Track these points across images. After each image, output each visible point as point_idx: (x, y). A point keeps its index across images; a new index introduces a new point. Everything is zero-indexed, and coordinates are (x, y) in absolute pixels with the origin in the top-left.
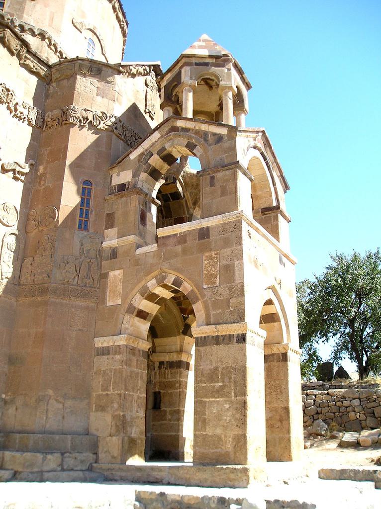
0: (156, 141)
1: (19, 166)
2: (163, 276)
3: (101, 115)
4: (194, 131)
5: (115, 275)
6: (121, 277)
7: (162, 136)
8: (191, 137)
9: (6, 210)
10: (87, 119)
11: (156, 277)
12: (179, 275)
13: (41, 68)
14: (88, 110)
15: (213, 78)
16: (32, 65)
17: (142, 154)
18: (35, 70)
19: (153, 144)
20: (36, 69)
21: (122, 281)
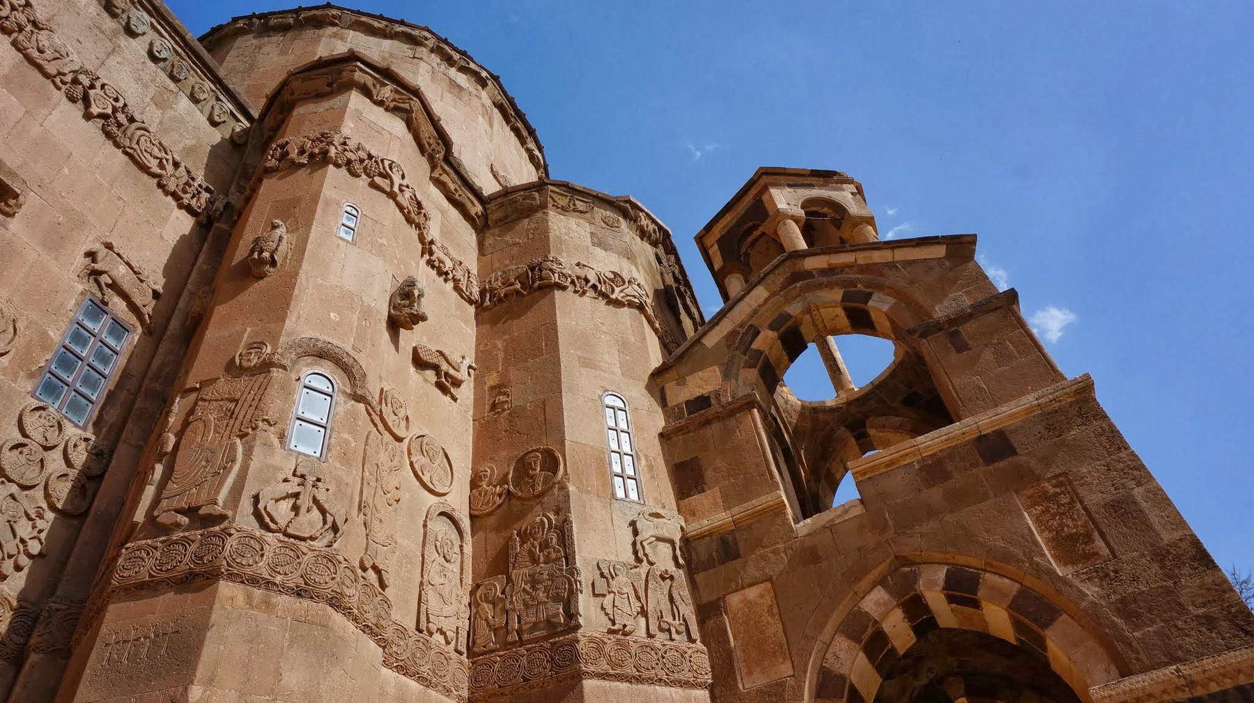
0: (760, 306)
1: (448, 361)
2: (905, 575)
3: (612, 276)
4: (855, 269)
5: (747, 602)
6: (768, 600)
7: (773, 294)
8: (853, 283)
9: (425, 453)
10: (587, 281)
11: (882, 582)
12: (961, 560)
13: (468, 198)
14: (584, 266)
15: (825, 210)
16: (452, 187)
17: (733, 334)
18: (457, 197)
19: (755, 312)
20: (460, 195)
21: (775, 610)
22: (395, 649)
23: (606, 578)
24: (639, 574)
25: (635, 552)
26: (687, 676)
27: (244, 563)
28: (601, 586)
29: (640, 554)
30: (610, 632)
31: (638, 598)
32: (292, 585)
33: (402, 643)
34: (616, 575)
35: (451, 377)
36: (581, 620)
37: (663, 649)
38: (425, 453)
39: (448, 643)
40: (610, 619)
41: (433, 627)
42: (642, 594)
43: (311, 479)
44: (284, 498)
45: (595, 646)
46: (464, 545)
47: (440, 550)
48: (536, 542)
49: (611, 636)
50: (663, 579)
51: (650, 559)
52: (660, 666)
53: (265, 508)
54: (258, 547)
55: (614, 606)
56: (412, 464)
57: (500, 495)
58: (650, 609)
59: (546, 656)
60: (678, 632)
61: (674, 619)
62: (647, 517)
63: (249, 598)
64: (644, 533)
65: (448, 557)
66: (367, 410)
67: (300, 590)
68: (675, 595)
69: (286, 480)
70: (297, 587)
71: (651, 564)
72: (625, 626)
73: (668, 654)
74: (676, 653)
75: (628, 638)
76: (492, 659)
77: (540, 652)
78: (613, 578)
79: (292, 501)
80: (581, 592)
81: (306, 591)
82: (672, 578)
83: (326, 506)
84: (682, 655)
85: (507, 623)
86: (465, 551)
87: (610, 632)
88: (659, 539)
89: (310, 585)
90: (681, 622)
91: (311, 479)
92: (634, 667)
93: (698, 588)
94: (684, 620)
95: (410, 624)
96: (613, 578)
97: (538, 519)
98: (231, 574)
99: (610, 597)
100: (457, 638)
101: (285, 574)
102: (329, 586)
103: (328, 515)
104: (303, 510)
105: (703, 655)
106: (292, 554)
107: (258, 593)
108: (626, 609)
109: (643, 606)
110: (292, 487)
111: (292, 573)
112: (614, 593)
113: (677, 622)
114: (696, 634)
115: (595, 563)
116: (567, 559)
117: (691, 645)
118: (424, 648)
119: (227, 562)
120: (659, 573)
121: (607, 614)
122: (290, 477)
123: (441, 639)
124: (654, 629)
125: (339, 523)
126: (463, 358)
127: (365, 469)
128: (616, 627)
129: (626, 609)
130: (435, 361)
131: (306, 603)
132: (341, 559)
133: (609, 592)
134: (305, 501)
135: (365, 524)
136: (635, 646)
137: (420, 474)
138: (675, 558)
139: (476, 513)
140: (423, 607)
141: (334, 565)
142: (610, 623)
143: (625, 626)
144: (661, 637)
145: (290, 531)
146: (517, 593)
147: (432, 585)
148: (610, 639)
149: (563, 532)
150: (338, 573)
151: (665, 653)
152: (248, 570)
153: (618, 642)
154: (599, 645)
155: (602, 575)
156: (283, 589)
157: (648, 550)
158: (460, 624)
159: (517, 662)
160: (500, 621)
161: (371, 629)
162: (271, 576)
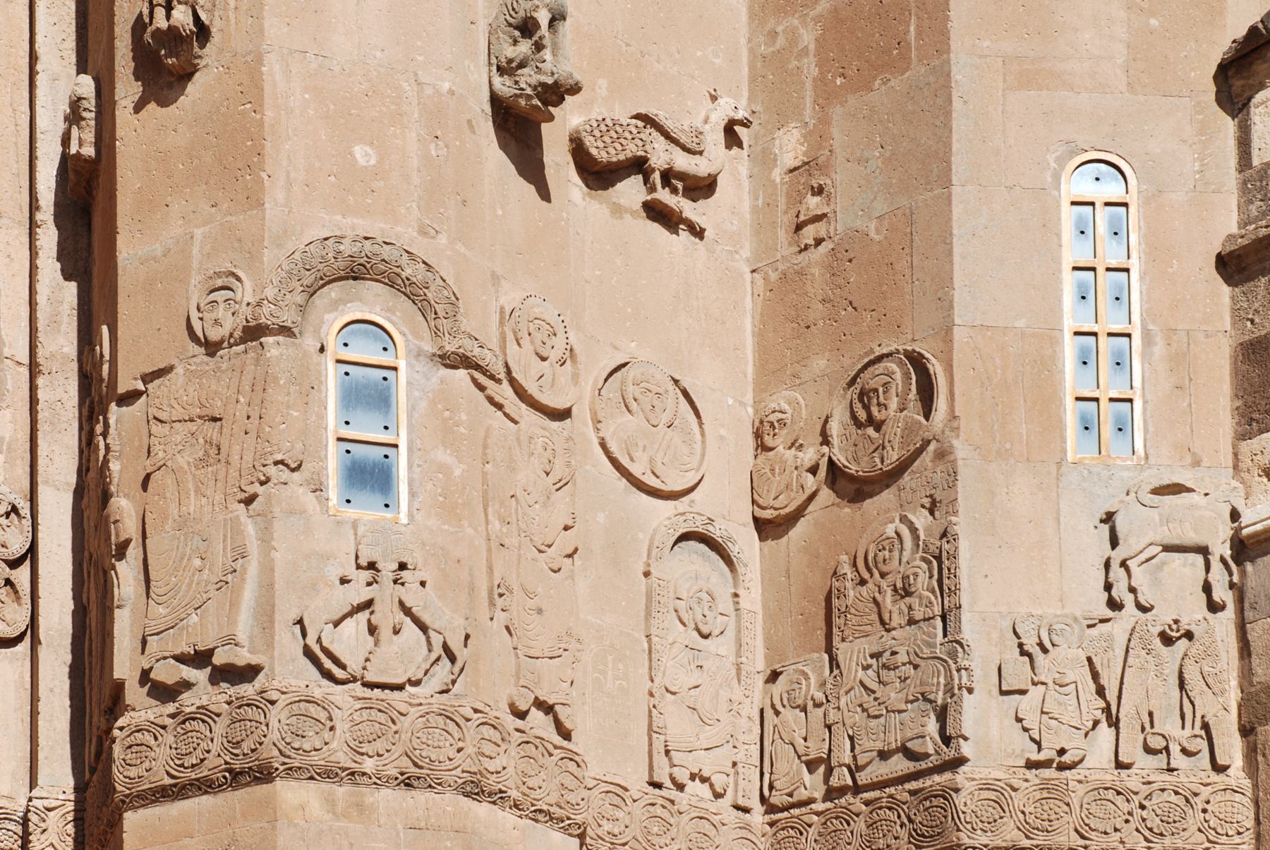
22: (607, 826)
23: (1030, 655)
24: (1109, 638)
26: (1192, 840)
27: (307, 747)
28: (1018, 673)
30: (1031, 765)
32: (394, 772)
33: (619, 814)
35: (682, 176)
36: (966, 749)
37: (1146, 790)
38: (633, 406)
39: (718, 796)
40: (1032, 740)
41: (682, 776)
42: (1110, 682)
43: (388, 568)
44: (350, 614)
45: (992, 795)
46: (741, 592)
47: (685, 619)
48: (884, 584)
49: (1030, 774)
50: (1167, 640)
52: (1132, 825)
53: (319, 640)
54: (323, 716)
56: (603, 445)
57: (813, 470)
58: (1126, 714)
63: (330, 803)
65: (705, 630)
66: (474, 381)
67: (409, 778)
69: (344, 581)
70: (402, 774)
72: (1062, 752)
73: (1155, 801)
74: (1173, 798)
75: (1067, 773)
78: (1045, 650)
79: (363, 617)
80: (970, 691)
81: (419, 778)
83: (426, 618)
84: (1187, 801)
86: (744, 603)
87: (1031, 765)
89: (421, 767)
90: (1198, 731)
91: (388, 568)
92: (1076, 831)
94: (1206, 726)
95: (636, 782)
96: (1045, 650)
97: (890, 530)
98: (290, 769)
99: (1036, 693)
100: (736, 784)
101: (379, 755)
102: (455, 763)
103: (432, 633)
104: (385, 632)
105: (1238, 797)
106: (382, 718)
107: (342, 791)
108: (1071, 716)
109: (1108, 705)
110: (358, 593)
111: (388, 751)
112: (1043, 683)
113: (1188, 731)
114: (1232, 749)
115: (1007, 625)
116: (944, 618)
117: (1215, 777)
118: (666, 815)
119: (280, 751)
121: (1026, 730)
122: (351, 572)
123: (703, 790)
124: (1131, 750)
125: (456, 646)
126: (714, 99)
127: (491, 517)
128: (1042, 757)
129: (1070, 714)
130: (632, 150)
131: (421, 797)
132: (468, 712)
134: (386, 614)
135: (507, 628)
136: (1081, 789)
137: (625, 461)
139: (767, 514)
140: (659, 746)
141: (457, 724)
144: (1146, 764)
145: (370, 677)
147: (674, 693)
149: (939, 559)
150: (468, 738)
151: (1149, 796)
152: (316, 759)
153: (1045, 786)
154: (998, 794)
156: (379, 781)
158: (739, 757)
160: (817, 749)
161: (548, 813)
162: (356, 762)
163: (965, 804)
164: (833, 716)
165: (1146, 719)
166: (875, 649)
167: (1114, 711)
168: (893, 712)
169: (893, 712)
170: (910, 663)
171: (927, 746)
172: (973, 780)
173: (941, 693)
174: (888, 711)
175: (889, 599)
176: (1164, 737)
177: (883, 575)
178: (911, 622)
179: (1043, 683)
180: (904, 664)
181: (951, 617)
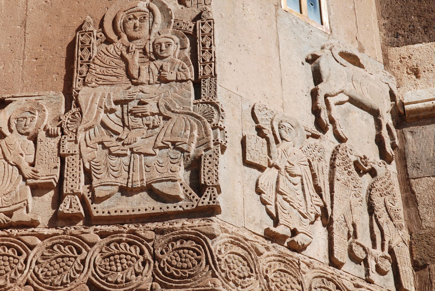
23: (268, 139)
25: (316, 111)
29: (324, 116)
31: (318, 190)
34: (282, 139)
36: (220, 199)
40: (269, 213)
49: (269, 244)
51: (339, 129)
55: (278, 191)
59: (142, 253)
60: (380, 271)
61: (374, 246)
62: (339, 58)
64: (332, 82)
68: (378, 202)
71: (341, 139)
72: (294, 232)
76: (27, 239)
77: (131, 244)
78: (277, 142)
82: (373, 173)
85: (62, 178)
88: (353, 101)
90: (386, 253)
93: (416, 203)
109: (325, 205)
112: (277, 167)
113: (378, 252)
120: (353, 158)
121: (264, 203)
133: (270, 166)
138: (379, 141)
142: (271, 222)
143: (294, 232)
146: (86, 130)
148: (267, 249)
149: (193, 37)
155: (260, 131)
157: (335, 110)
159: (79, 252)
163: (220, 252)
164: (68, 147)
165: (352, 229)
166: (121, 97)
167: (330, 213)
168: (140, 153)
169: (140, 153)
170: (160, 114)
171: (178, 190)
172: (226, 231)
173: (193, 146)
174: (132, 152)
175: (137, 59)
176: (364, 249)
177: (131, 39)
178: (162, 80)
179: (277, 167)
180: (153, 114)
181: (206, 85)
